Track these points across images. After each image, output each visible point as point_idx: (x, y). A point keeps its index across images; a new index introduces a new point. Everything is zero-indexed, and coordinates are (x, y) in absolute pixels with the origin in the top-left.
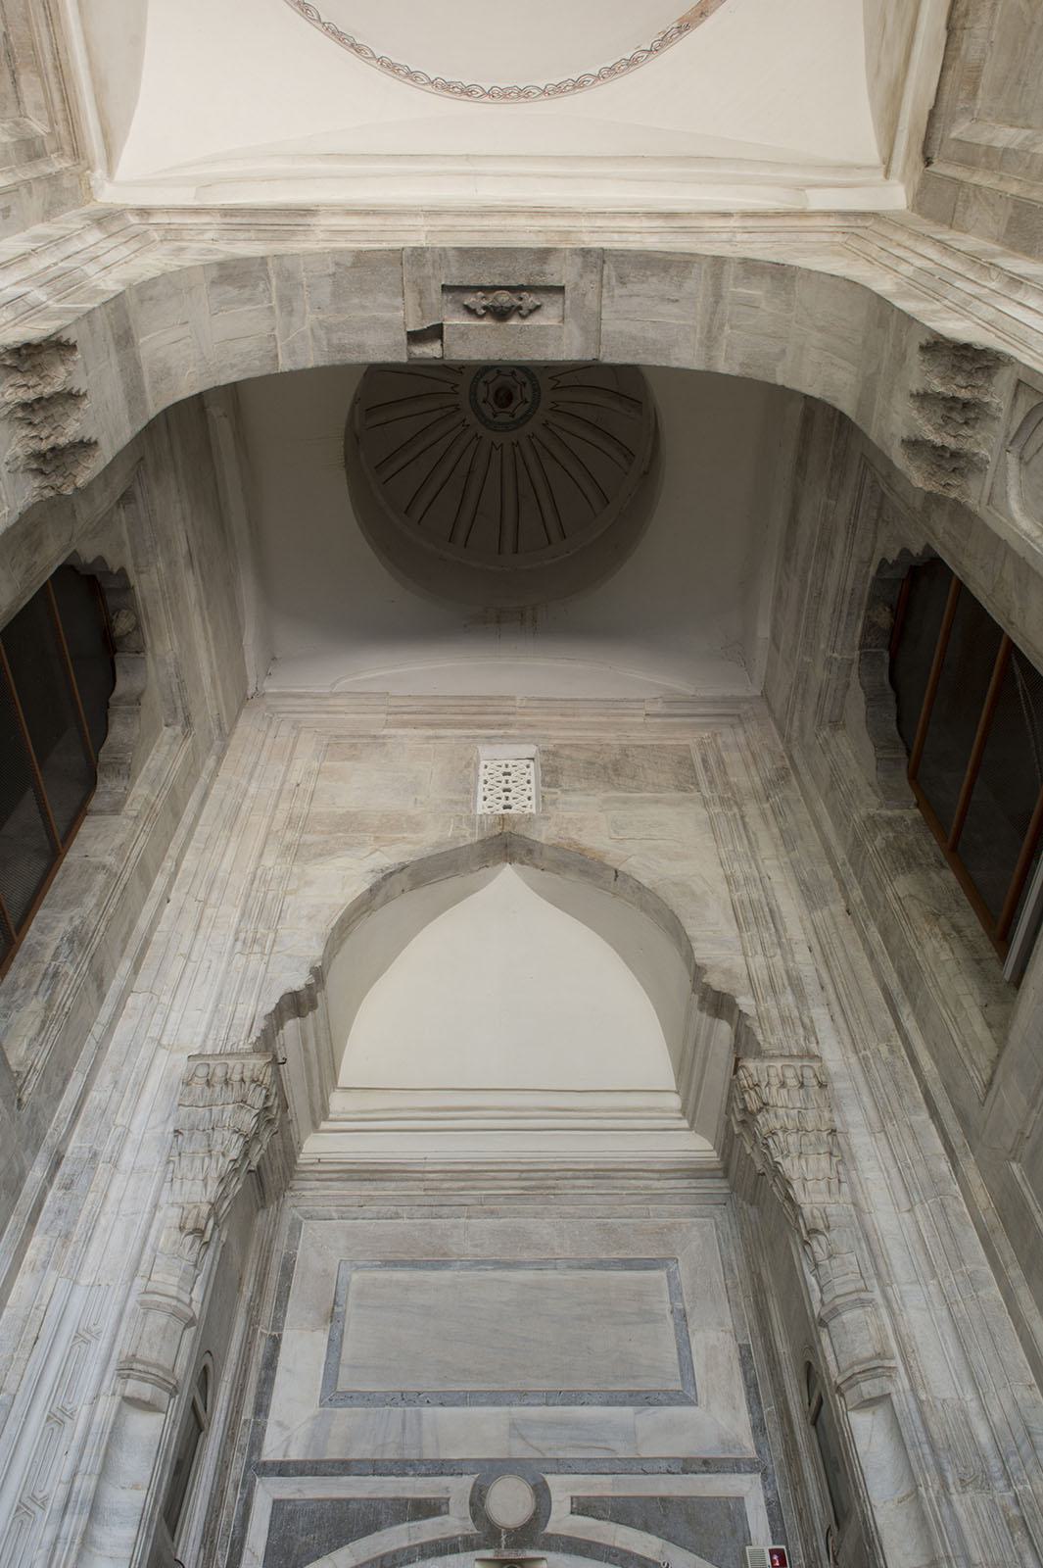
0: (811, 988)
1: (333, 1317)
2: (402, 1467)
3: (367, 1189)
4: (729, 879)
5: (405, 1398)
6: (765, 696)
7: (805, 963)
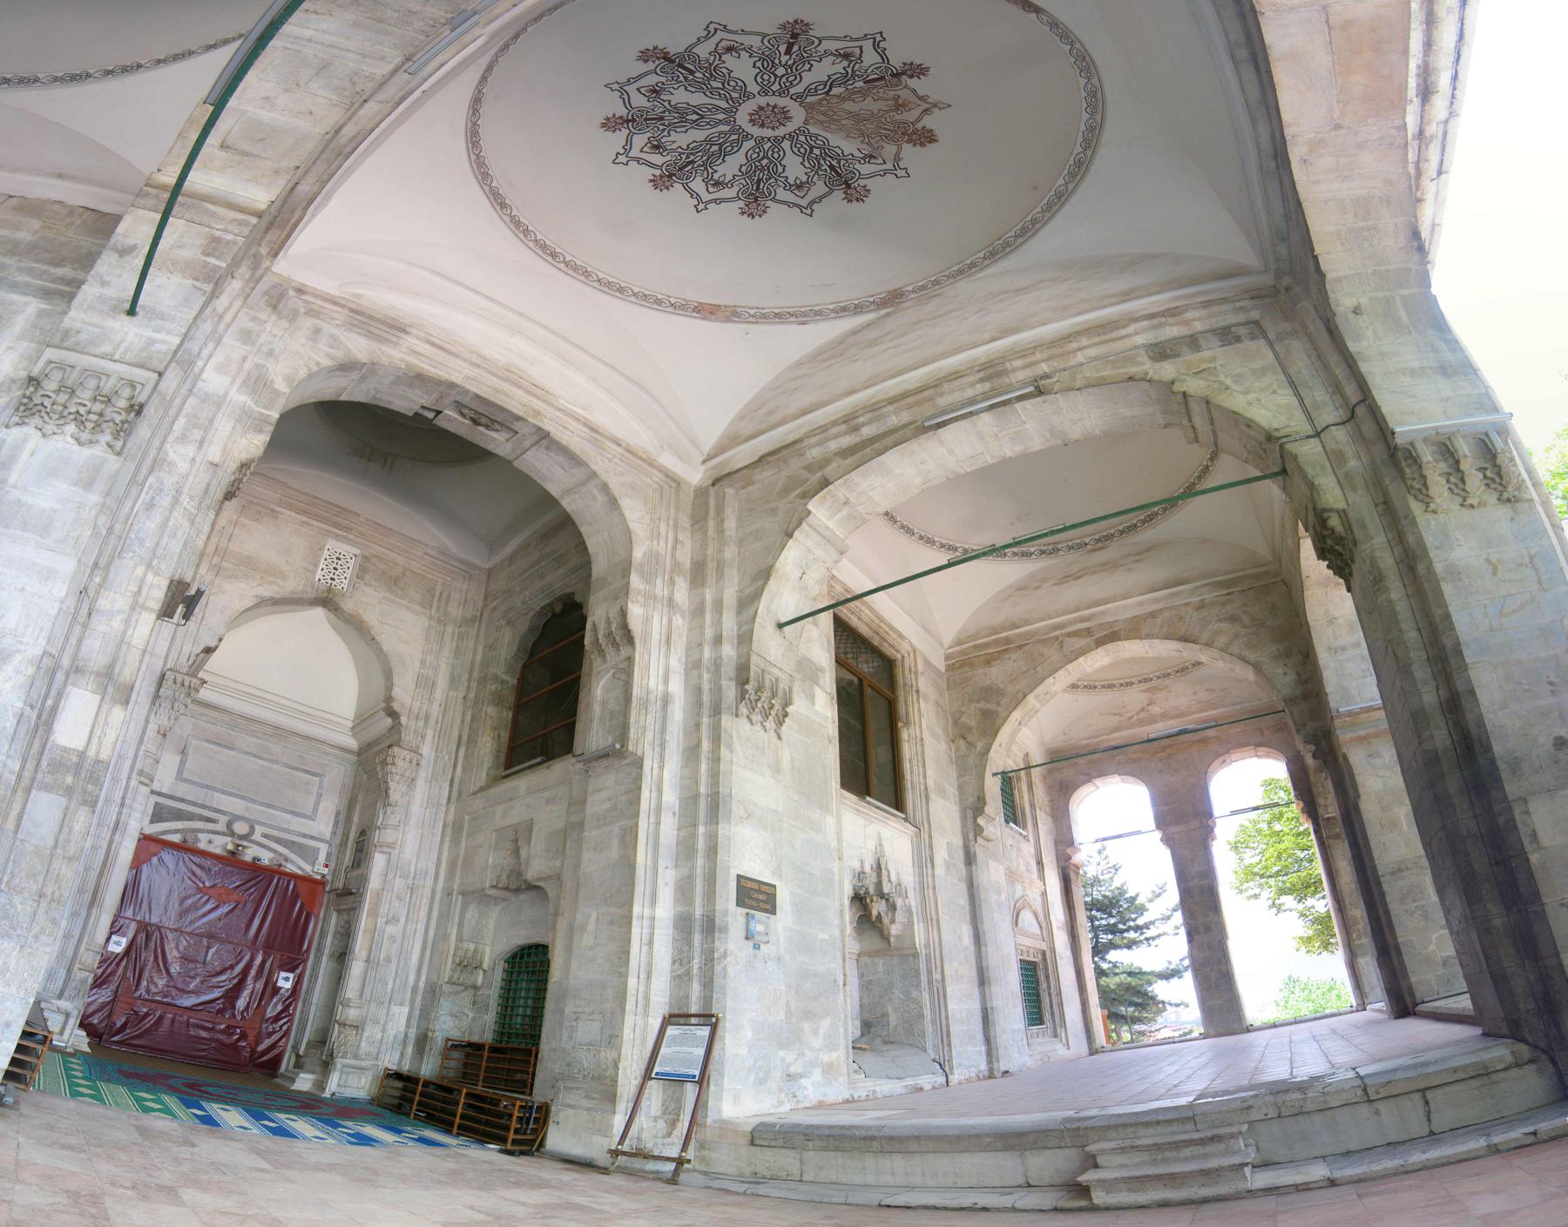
0: (432, 721)
1: (183, 752)
2: (204, 807)
3: (205, 711)
4: (423, 662)
5: (208, 787)
6: (490, 572)
7: (435, 710)
